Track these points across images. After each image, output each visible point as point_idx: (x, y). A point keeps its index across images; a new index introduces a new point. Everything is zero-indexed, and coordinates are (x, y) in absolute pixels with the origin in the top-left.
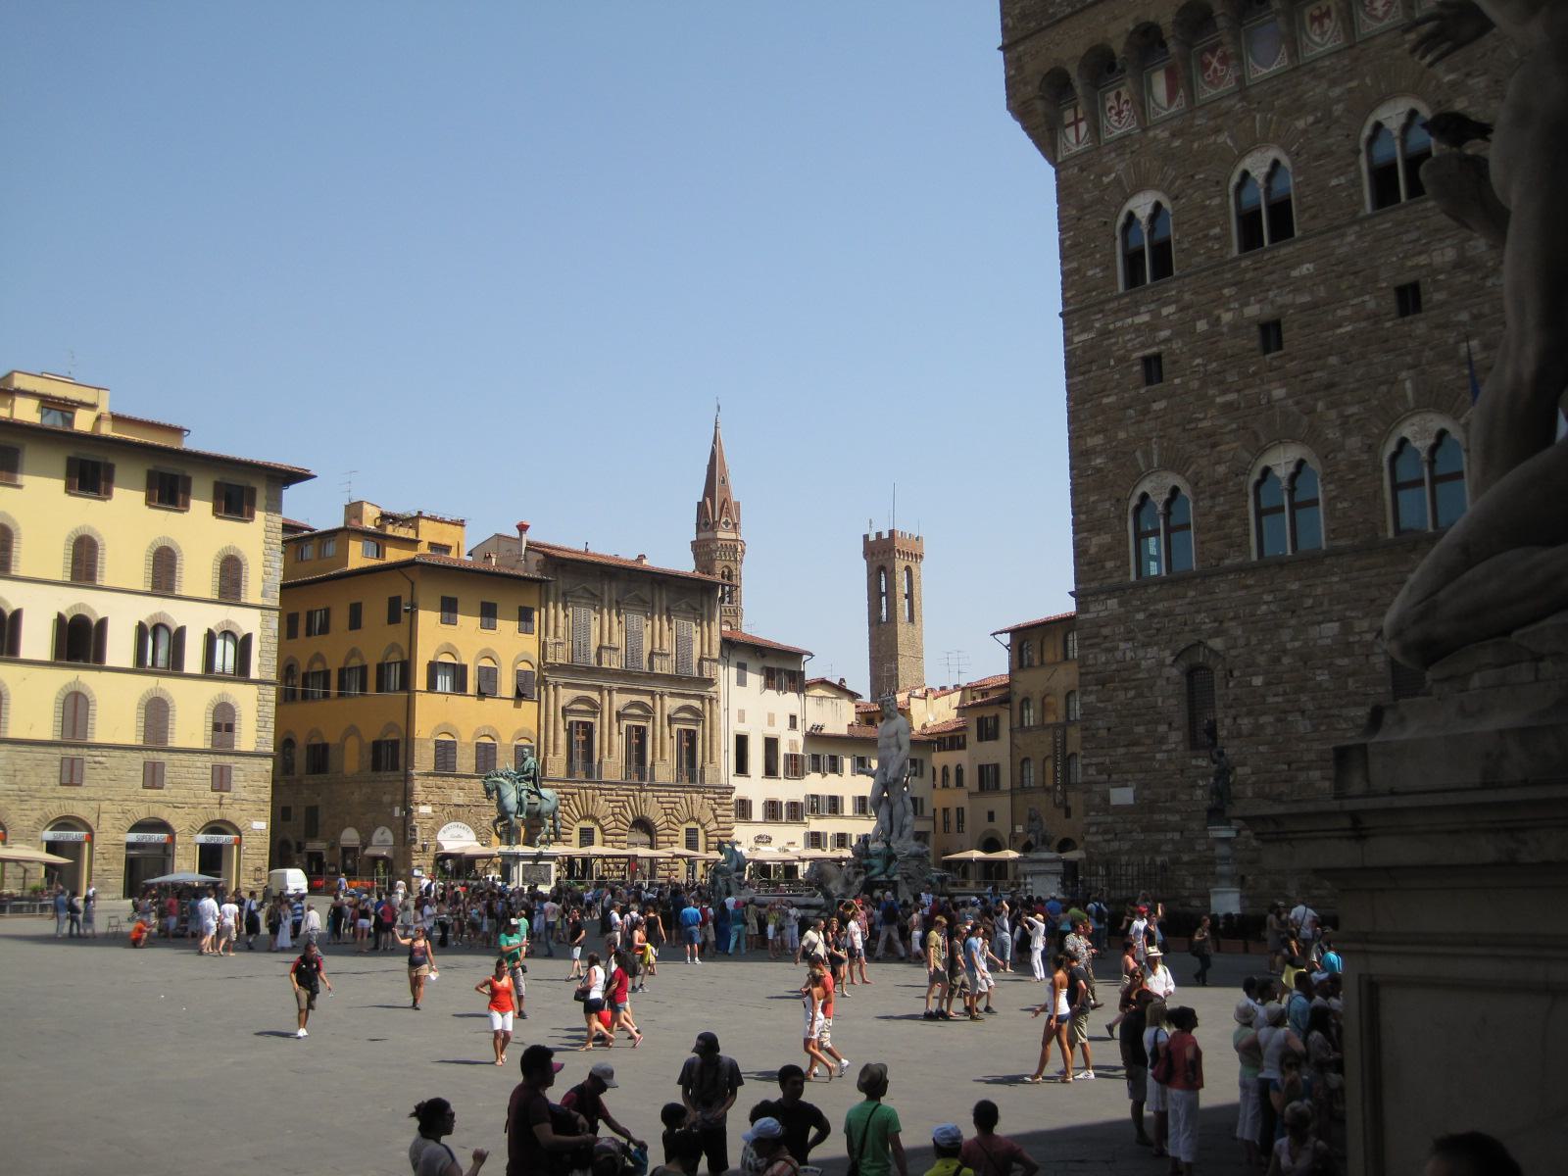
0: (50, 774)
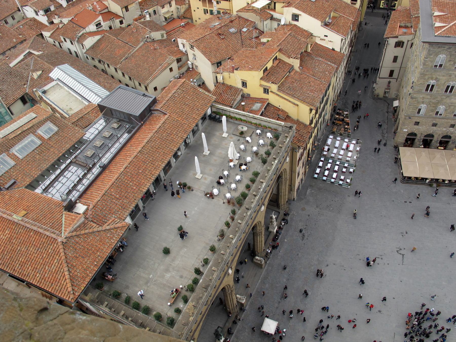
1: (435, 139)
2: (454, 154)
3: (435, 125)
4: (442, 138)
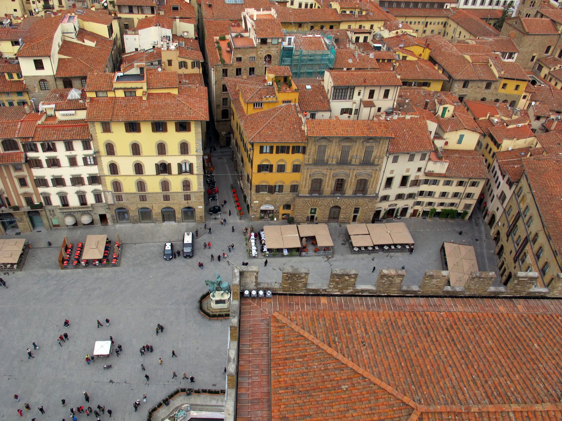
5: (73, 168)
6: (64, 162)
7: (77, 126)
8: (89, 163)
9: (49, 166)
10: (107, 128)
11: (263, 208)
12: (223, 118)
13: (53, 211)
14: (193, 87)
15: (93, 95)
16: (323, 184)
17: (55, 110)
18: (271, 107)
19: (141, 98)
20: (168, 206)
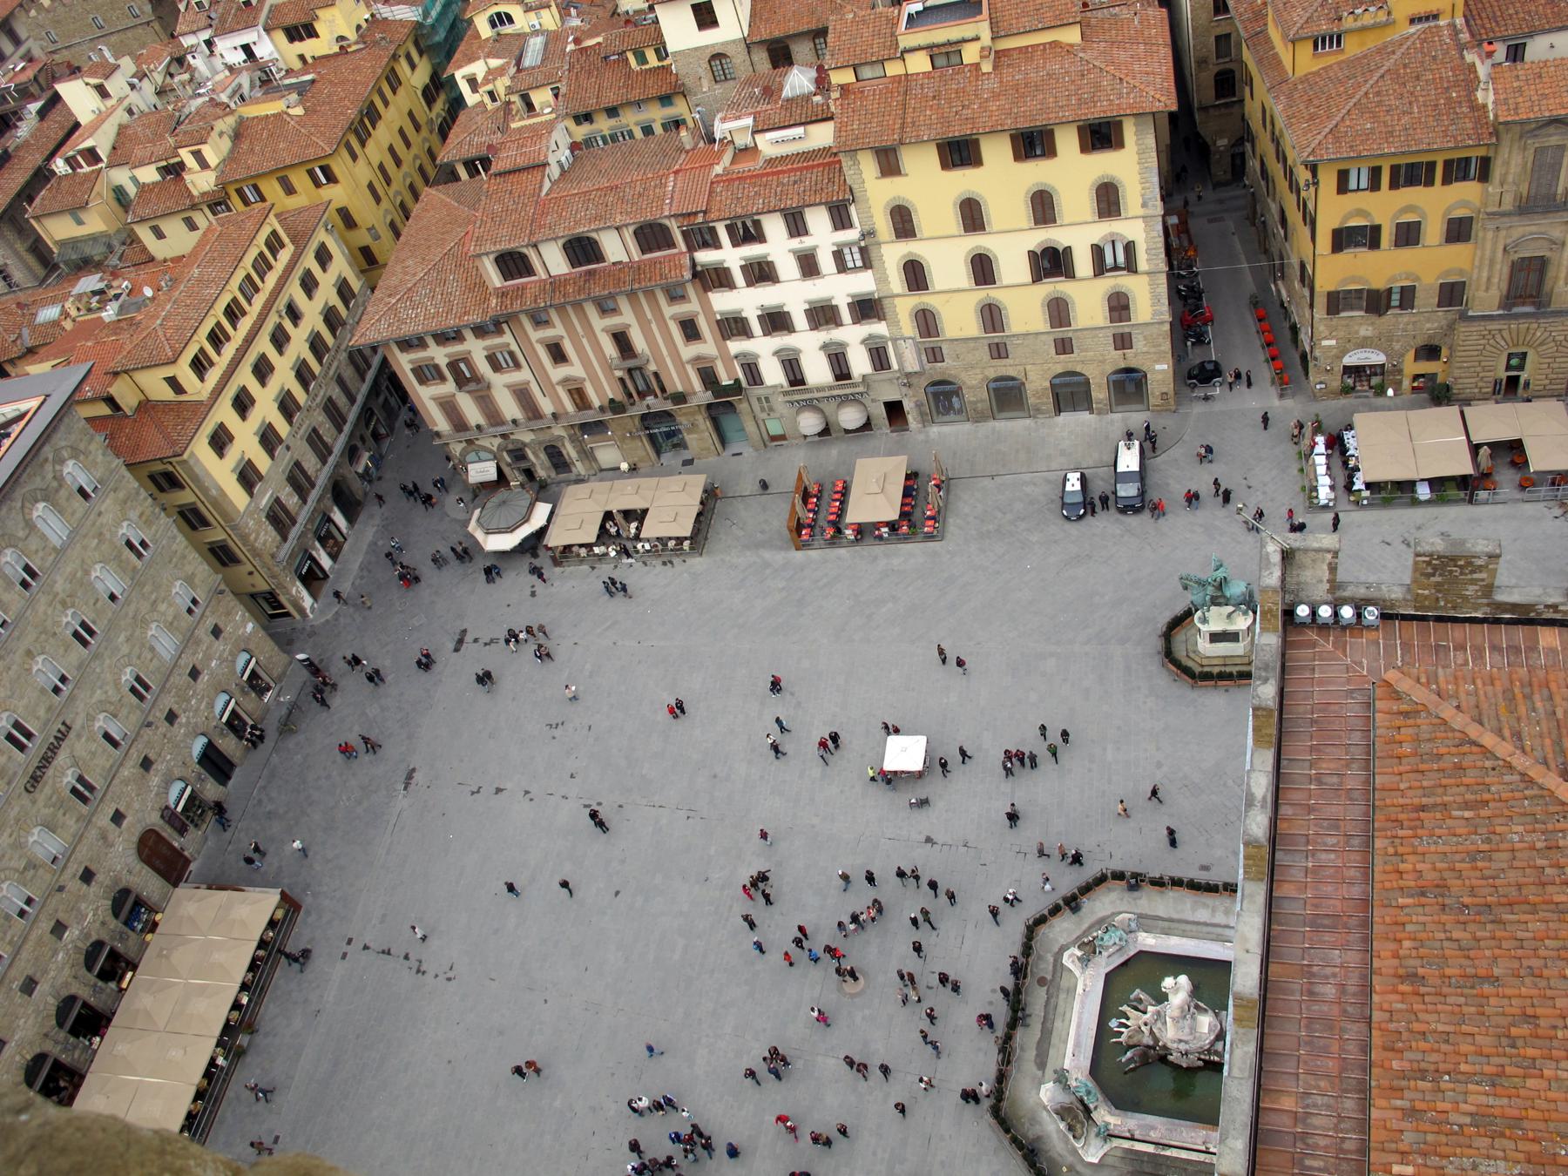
0: (984, 353)
1: (84, 993)
2: (162, 950)
3: (29, 986)
4: (89, 968)
5: (809, 283)
6: (787, 267)
7: (813, 167)
8: (850, 265)
9: (750, 284)
10: (889, 165)
11: (1352, 359)
12: (1217, 98)
13: (767, 399)
14: (1124, 13)
15: (847, 77)
16: (1551, 273)
17: (754, 132)
18: (1372, 41)
19: (977, 66)
20: (1070, 368)
